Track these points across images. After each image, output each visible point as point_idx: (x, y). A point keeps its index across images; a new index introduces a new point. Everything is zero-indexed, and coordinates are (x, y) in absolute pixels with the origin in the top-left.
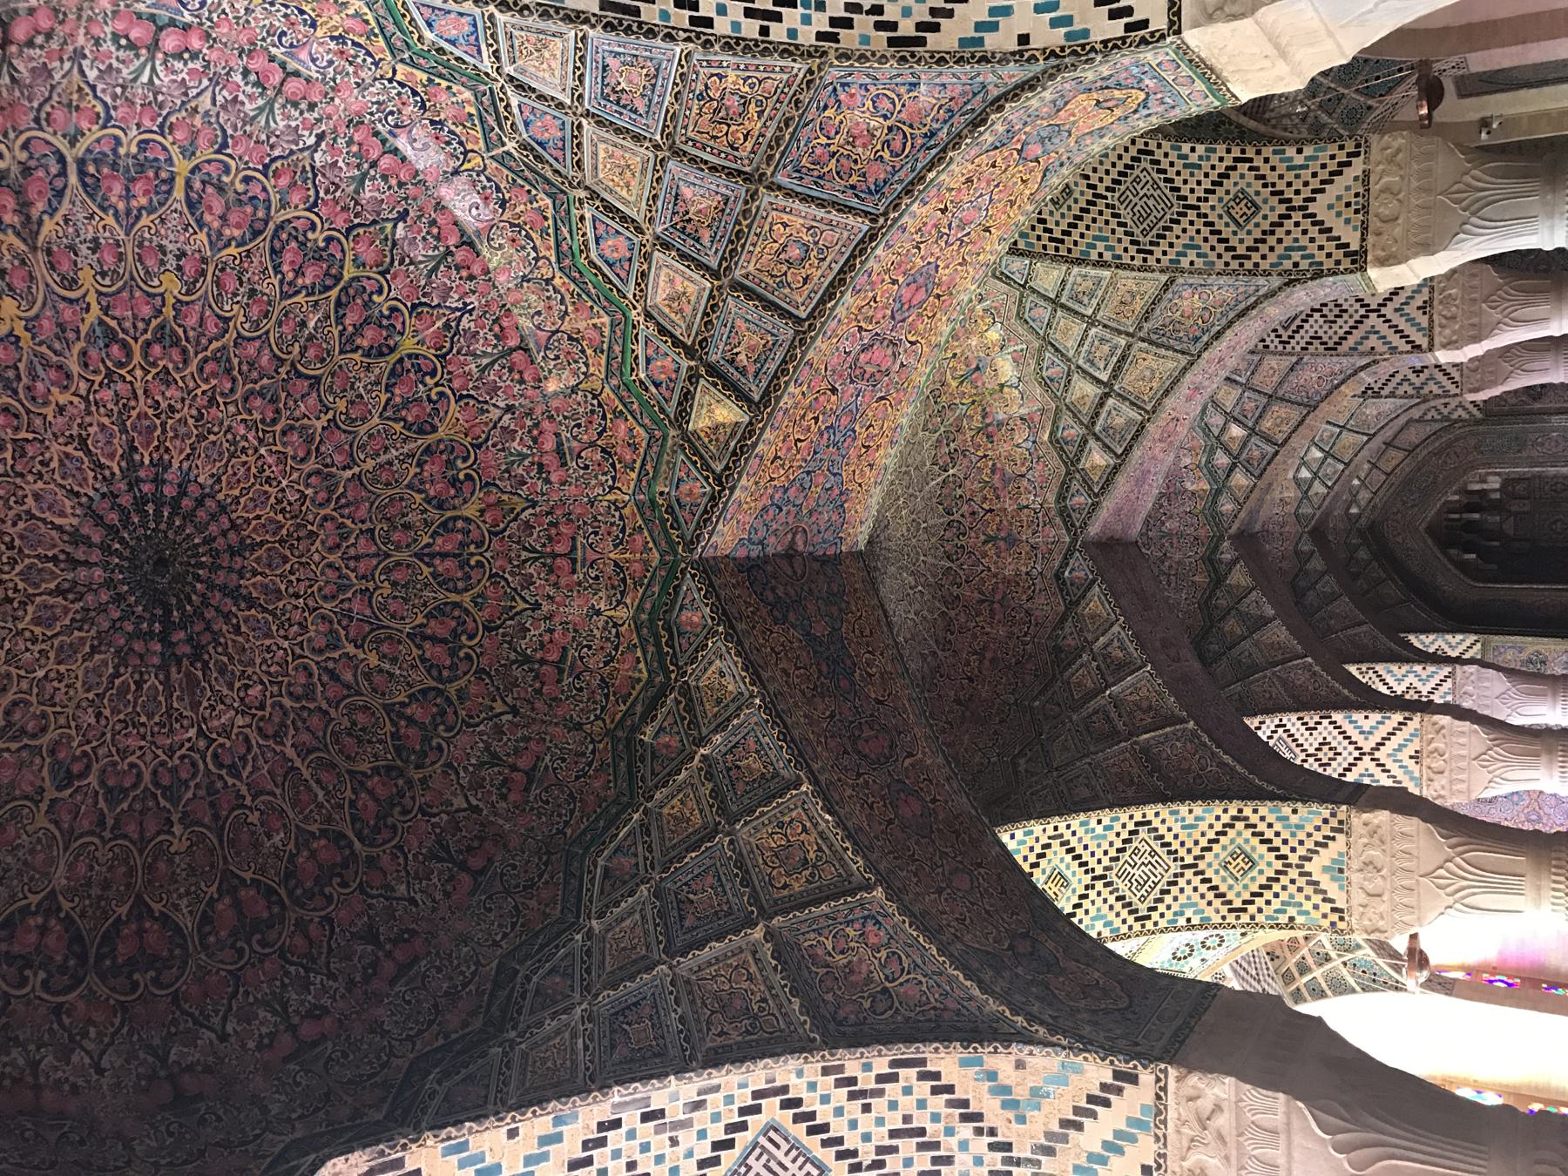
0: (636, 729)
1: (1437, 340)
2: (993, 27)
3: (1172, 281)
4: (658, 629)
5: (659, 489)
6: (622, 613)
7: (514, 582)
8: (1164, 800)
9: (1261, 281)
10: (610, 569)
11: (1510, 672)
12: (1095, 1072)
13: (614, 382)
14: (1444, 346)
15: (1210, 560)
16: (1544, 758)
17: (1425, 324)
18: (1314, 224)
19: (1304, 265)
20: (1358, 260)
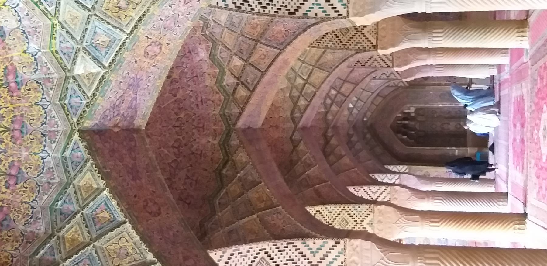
0: (221, 170)
1: (395, 64)
2: (310, 11)
3: (325, 51)
4: (225, 145)
5: (226, 111)
6: (216, 142)
7: (191, 133)
8: (323, 204)
9: (349, 52)
10: (213, 131)
11: (418, 177)
12: (331, 242)
13: (217, 85)
14: (397, 66)
15: (325, 135)
16: (426, 199)
17: (391, 59)
18: (364, 36)
19: (361, 48)
20: (375, 47)
